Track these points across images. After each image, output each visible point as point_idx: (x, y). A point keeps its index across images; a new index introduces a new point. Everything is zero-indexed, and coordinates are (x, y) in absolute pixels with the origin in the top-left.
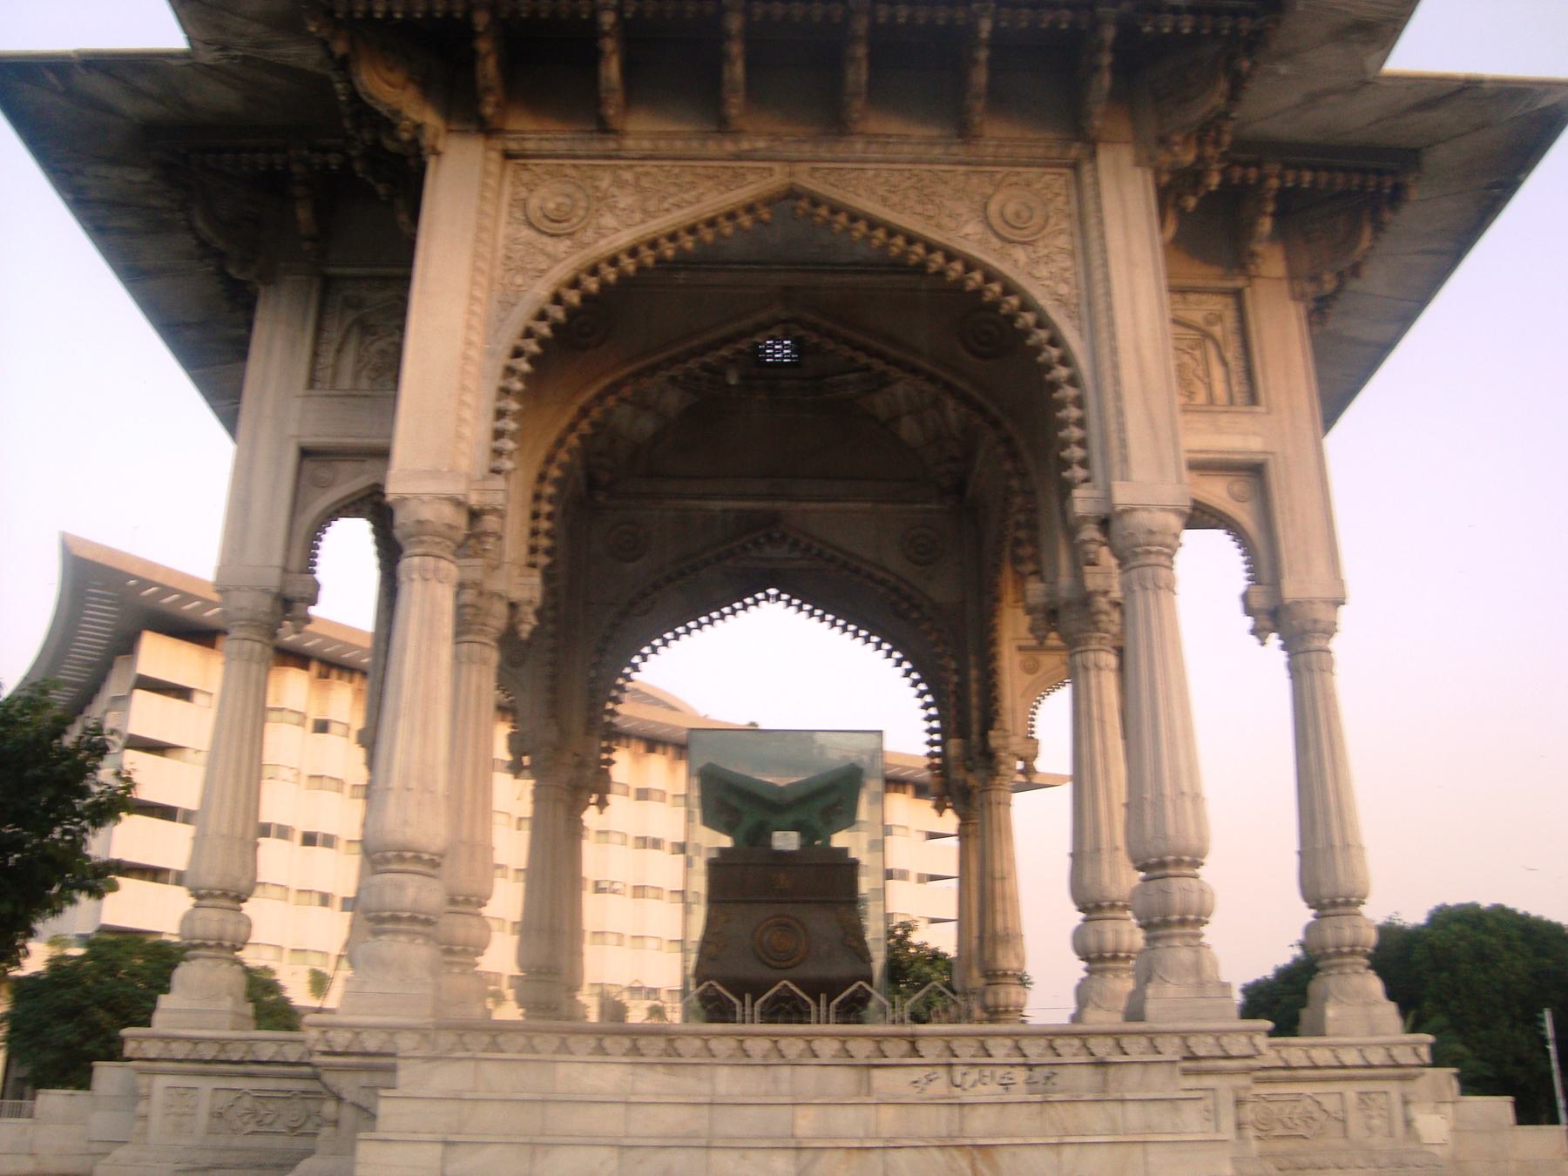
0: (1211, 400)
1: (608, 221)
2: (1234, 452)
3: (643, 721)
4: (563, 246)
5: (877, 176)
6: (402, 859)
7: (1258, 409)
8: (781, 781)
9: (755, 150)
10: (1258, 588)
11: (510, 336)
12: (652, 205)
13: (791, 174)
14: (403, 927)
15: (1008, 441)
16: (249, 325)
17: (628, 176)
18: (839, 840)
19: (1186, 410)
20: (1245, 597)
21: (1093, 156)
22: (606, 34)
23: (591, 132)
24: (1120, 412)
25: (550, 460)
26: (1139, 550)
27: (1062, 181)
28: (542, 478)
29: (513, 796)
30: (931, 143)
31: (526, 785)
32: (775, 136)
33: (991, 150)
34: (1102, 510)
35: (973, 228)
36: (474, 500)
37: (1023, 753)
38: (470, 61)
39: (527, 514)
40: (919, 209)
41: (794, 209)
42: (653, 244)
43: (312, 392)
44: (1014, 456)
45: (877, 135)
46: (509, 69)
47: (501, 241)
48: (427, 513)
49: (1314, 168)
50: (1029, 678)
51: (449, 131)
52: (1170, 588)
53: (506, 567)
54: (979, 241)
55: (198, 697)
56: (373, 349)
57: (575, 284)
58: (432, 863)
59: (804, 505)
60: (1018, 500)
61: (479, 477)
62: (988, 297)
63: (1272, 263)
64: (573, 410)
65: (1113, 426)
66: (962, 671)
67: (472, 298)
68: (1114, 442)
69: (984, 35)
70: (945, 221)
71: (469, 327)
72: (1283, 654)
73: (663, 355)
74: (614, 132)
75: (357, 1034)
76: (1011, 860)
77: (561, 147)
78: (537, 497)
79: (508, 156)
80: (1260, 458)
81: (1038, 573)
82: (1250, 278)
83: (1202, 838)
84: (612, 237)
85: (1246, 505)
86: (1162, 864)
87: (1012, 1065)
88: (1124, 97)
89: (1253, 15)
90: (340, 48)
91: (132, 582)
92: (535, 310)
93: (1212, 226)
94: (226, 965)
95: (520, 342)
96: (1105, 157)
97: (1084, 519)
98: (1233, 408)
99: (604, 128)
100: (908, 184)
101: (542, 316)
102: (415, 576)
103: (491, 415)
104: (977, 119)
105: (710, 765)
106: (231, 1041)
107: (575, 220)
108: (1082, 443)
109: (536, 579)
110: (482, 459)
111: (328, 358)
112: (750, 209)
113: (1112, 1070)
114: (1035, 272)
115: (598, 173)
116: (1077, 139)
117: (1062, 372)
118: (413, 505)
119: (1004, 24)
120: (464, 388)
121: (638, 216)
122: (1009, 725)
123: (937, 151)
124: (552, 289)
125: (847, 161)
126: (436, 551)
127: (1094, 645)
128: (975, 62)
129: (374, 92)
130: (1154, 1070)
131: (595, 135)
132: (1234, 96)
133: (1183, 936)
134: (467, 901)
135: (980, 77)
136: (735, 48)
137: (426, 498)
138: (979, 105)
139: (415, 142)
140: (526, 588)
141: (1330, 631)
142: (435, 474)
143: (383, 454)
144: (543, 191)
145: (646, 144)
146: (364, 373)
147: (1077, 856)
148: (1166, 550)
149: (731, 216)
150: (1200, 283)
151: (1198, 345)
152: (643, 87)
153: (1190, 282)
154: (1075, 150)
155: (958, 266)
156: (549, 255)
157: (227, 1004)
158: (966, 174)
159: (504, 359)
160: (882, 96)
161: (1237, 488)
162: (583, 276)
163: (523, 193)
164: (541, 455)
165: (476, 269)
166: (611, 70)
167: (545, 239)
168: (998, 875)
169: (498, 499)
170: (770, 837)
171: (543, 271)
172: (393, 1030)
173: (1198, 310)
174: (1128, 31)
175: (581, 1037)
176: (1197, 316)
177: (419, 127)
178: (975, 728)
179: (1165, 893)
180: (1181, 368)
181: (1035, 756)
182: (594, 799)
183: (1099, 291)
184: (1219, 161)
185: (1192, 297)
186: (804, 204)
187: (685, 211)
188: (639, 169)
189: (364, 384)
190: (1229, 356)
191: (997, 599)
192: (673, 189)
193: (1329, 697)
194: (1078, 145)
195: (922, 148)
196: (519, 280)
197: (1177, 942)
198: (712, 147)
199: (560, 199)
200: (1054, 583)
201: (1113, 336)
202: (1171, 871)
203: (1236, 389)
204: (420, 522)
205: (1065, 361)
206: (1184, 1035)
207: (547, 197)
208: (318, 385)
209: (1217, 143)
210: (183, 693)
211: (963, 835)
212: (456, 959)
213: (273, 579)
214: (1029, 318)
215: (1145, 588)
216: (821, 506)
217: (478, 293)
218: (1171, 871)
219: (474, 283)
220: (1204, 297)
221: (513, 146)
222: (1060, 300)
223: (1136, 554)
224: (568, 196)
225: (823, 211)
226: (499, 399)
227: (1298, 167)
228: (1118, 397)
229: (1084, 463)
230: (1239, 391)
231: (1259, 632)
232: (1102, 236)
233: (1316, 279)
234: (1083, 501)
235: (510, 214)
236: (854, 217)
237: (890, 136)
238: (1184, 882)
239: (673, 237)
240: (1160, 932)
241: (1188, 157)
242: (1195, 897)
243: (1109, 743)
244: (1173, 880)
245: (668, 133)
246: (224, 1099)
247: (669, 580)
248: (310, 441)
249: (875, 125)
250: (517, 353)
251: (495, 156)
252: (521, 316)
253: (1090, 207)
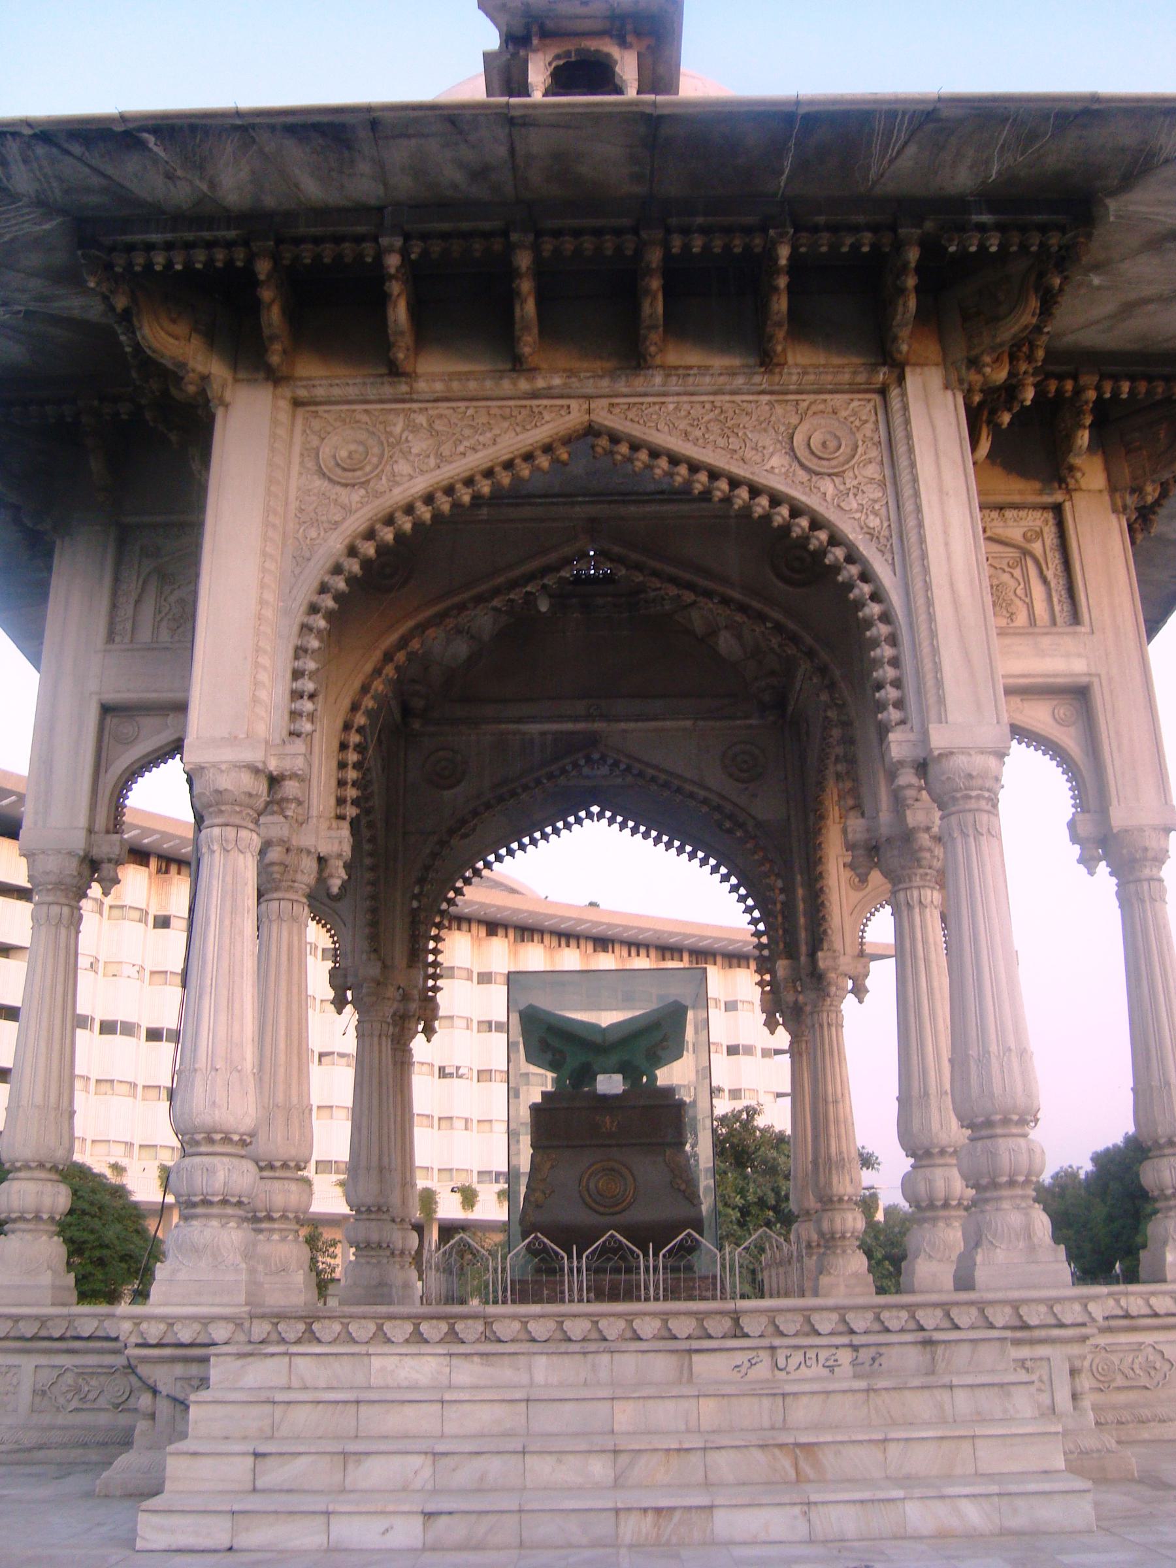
0: (1032, 620)
1: (403, 467)
2: (1055, 676)
3: (482, 905)
4: (357, 495)
5: (677, 409)
6: (211, 1141)
7: (1079, 629)
8: (607, 1018)
9: (550, 388)
10: (1087, 816)
11: (305, 591)
12: (446, 450)
13: (589, 412)
14: (215, 1210)
15: (823, 670)
16: (49, 569)
17: (421, 419)
18: (666, 1076)
19: (1002, 633)
20: (1072, 825)
21: (901, 380)
22: (392, 277)
23: (381, 376)
24: (935, 651)
25: (355, 708)
26: (959, 795)
27: (870, 406)
28: (347, 727)
29: (335, 1031)
30: (732, 373)
31: (350, 1014)
32: (571, 373)
33: (794, 378)
34: (920, 754)
35: (778, 461)
36: (273, 765)
37: (852, 972)
38: (255, 308)
39: (334, 764)
40: (721, 442)
41: (593, 447)
42: (449, 490)
43: (109, 647)
44: (832, 686)
45: (676, 368)
46: (295, 318)
47: (293, 493)
48: (225, 782)
49: (1132, 378)
50: (860, 895)
51: (236, 380)
52: (994, 834)
53: (315, 820)
54: (786, 474)
56: (172, 599)
57: (370, 535)
58: (241, 1144)
59: (623, 725)
60: (836, 733)
61: (278, 741)
62: (796, 532)
63: (1091, 474)
64: (378, 655)
65: (928, 666)
66: (788, 890)
67: (264, 554)
68: (930, 682)
69: (783, 262)
70: (749, 454)
71: (262, 586)
72: (1114, 880)
73: (466, 595)
74: (404, 374)
75: (172, 1325)
76: (844, 1083)
77: (352, 392)
78: (343, 746)
79: (297, 403)
80: (1084, 680)
81: (858, 807)
82: (1069, 492)
83: (1029, 1094)
84: (406, 486)
85: (1072, 730)
86: (989, 1124)
87: (837, 1347)
88: (931, 318)
89: (1063, 229)
90: (121, 302)
92: (329, 564)
93: (1024, 442)
94: (45, 1238)
95: (315, 598)
96: (913, 380)
97: (901, 763)
98: (1055, 630)
99: (394, 371)
100: (712, 415)
101: (337, 570)
102: (216, 847)
103: (289, 675)
104: (779, 348)
105: (531, 1007)
106: (51, 1318)
107: (368, 468)
108: (897, 684)
109: (345, 832)
110: (282, 723)
111: (126, 610)
112: (548, 449)
113: (940, 1350)
114: (842, 504)
115: (391, 417)
116: (885, 361)
117: (875, 609)
118: (210, 774)
119: (803, 250)
120: (258, 650)
121: (432, 462)
122: (838, 946)
123: (740, 381)
124: (347, 542)
125: (645, 395)
126: (238, 821)
127: (917, 881)
128: (776, 289)
129: (155, 344)
130: (983, 1349)
131: (386, 379)
132: (1046, 311)
133: (1012, 1197)
134: (285, 1166)
135: (781, 304)
136: (526, 286)
137: (223, 767)
138: (781, 334)
139: (203, 392)
140: (335, 841)
141: (1160, 858)
142: (232, 741)
143: (181, 708)
144: (333, 440)
145: (439, 386)
146: (164, 623)
147: (905, 1101)
148: (986, 794)
149: (528, 457)
150: (1017, 499)
151: (1020, 563)
152: (431, 328)
154: (881, 375)
155: (764, 501)
156: (343, 507)
157: (46, 1278)
158: (769, 403)
159: (299, 617)
160: (679, 327)
161: (1062, 711)
162: (378, 526)
163: (315, 442)
164: (346, 703)
165: (267, 524)
166: (399, 313)
167: (338, 489)
168: (830, 1099)
169: (299, 764)
170: (594, 1079)
171: (336, 523)
172: (206, 1321)
173: (1015, 527)
174: (931, 248)
175: (398, 1322)
176: (1015, 533)
177: (205, 378)
178: (803, 949)
179: (993, 1154)
180: (997, 589)
181: (867, 976)
182: (420, 1028)
183: (911, 522)
184: (1033, 375)
185: (1009, 514)
186: (604, 442)
187: (480, 455)
188: (430, 412)
189: (165, 636)
190: (1050, 574)
191: (822, 817)
192: (467, 432)
193: (1161, 928)
194: (885, 369)
195: (722, 379)
196: (313, 533)
197: (1006, 1205)
198: (506, 385)
199: (353, 447)
200: (875, 818)
201: (926, 570)
202: (999, 1131)
203: (1057, 608)
204: (218, 792)
205: (876, 597)
206: (1015, 1305)
207: (339, 444)
208: (118, 639)
209: (1030, 358)
211: (795, 1051)
212: (276, 1226)
213: (78, 842)
214: (839, 553)
215: (965, 835)
216: (640, 724)
217: (269, 549)
218: (999, 1131)
219: (265, 539)
220: (1022, 513)
221: (302, 393)
222: (871, 534)
223: (954, 799)
224: (361, 443)
225: (624, 449)
226: (296, 657)
227: (1116, 378)
228: (933, 634)
229: (899, 704)
230: (1061, 609)
231: (1088, 862)
232: (913, 465)
233: (1137, 490)
234: (899, 744)
235: (302, 463)
236: (655, 453)
237: (691, 368)
238: (1011, 1143)
239: (469, 482)
240: (988, 1195)
241: (1000, 375)
242: (1024, 1159)
243: (936, 984)
244: (1001, 1140)
245: (460, 374)
246: (46, 1377)
247: (488, 806)
248: (112, 697)
250: (313, 609)
251: (284, 404)
252: (315, 572)
253: (899, 434)
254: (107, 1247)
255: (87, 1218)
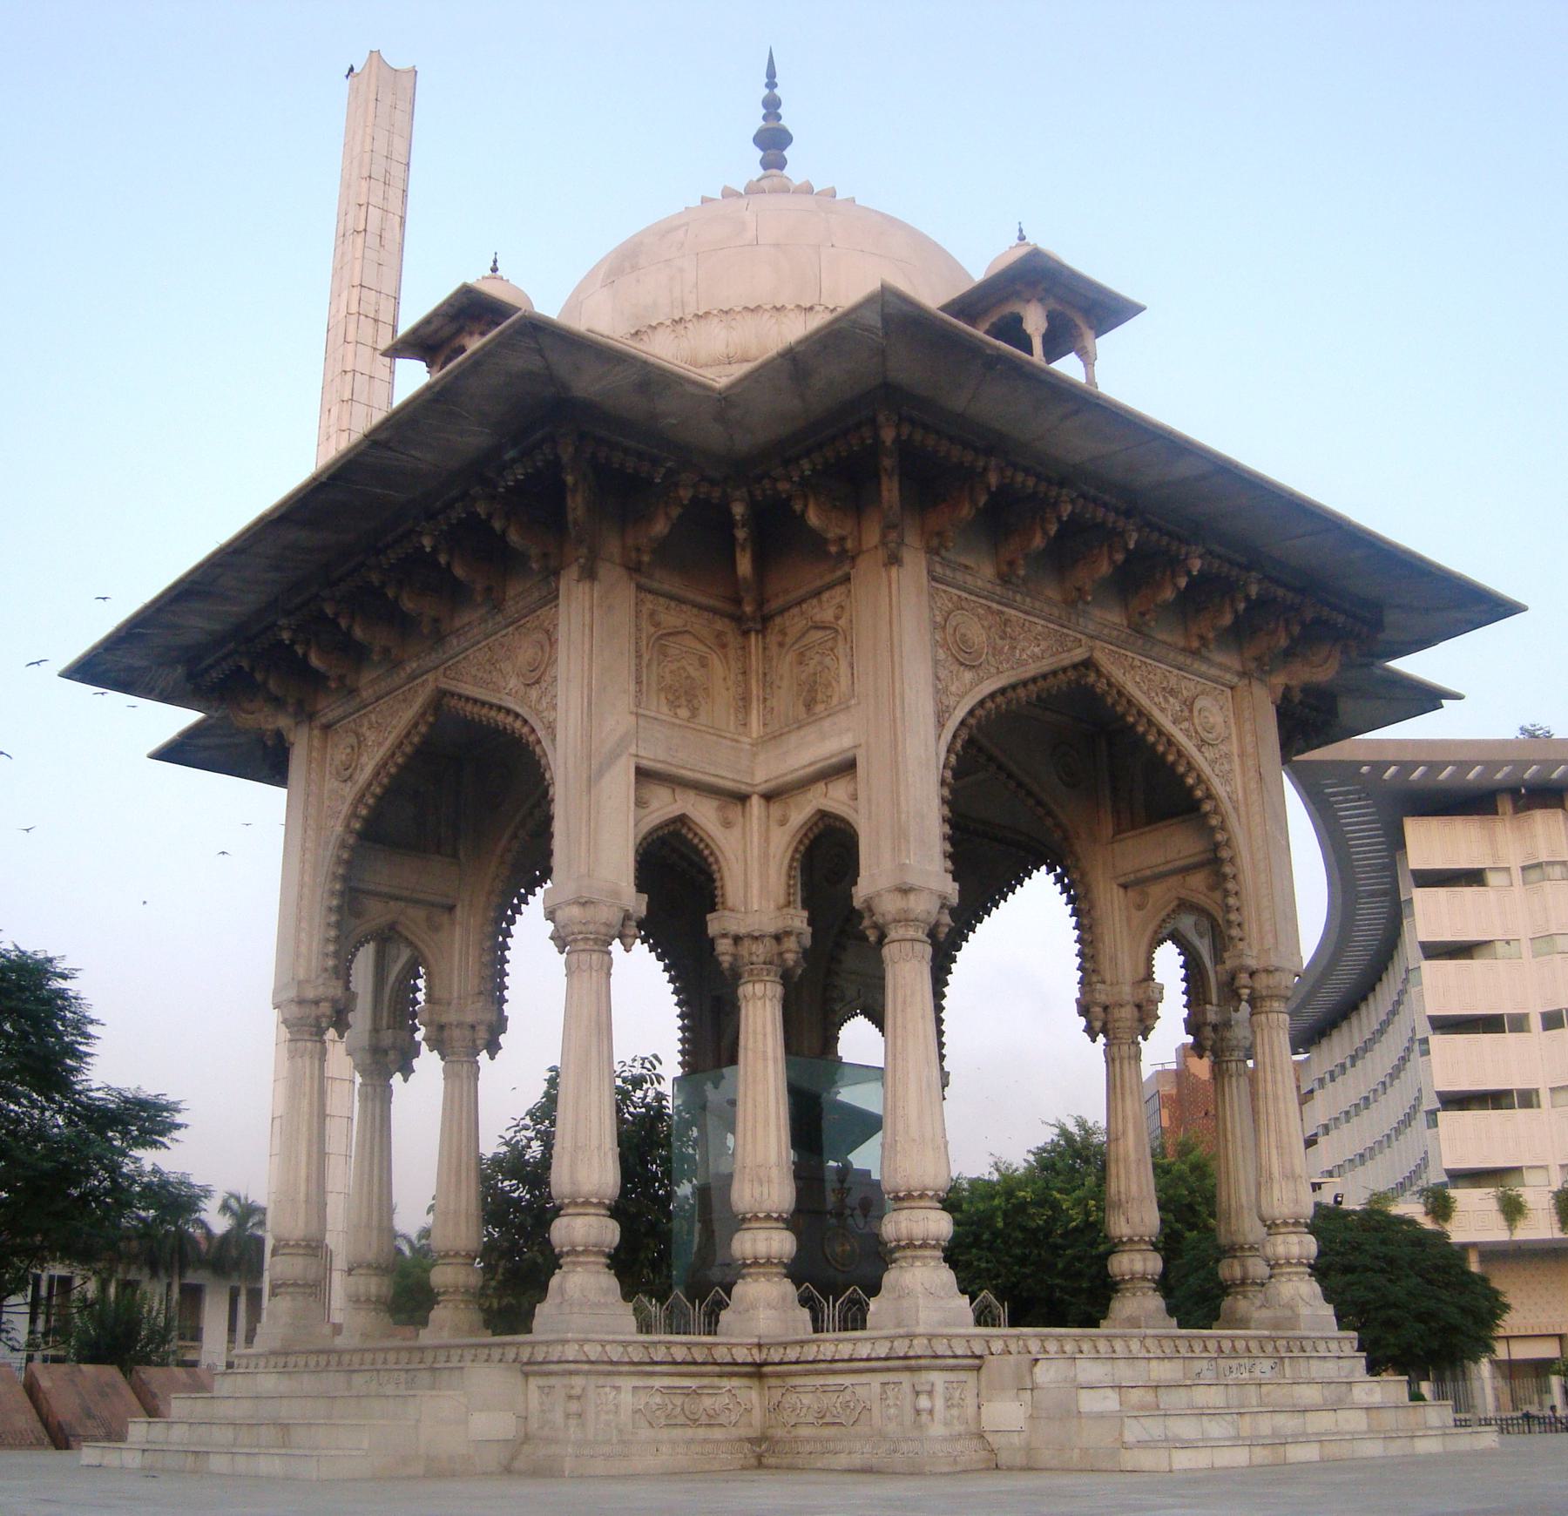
30: (483, 620)
55: (1492, 878)
80: (849, 754)
91: (1365, 769)
150: (828, 578)
153: (818, 583)
185: (825, 596)
210: (1473, 878)
221: (324, 720)
249: (457, 624)
251: (316, 732)
254: (1395, 1305)
255: (1369, 1274)
